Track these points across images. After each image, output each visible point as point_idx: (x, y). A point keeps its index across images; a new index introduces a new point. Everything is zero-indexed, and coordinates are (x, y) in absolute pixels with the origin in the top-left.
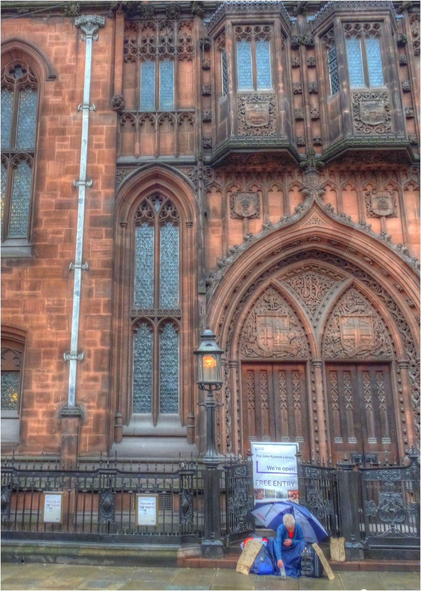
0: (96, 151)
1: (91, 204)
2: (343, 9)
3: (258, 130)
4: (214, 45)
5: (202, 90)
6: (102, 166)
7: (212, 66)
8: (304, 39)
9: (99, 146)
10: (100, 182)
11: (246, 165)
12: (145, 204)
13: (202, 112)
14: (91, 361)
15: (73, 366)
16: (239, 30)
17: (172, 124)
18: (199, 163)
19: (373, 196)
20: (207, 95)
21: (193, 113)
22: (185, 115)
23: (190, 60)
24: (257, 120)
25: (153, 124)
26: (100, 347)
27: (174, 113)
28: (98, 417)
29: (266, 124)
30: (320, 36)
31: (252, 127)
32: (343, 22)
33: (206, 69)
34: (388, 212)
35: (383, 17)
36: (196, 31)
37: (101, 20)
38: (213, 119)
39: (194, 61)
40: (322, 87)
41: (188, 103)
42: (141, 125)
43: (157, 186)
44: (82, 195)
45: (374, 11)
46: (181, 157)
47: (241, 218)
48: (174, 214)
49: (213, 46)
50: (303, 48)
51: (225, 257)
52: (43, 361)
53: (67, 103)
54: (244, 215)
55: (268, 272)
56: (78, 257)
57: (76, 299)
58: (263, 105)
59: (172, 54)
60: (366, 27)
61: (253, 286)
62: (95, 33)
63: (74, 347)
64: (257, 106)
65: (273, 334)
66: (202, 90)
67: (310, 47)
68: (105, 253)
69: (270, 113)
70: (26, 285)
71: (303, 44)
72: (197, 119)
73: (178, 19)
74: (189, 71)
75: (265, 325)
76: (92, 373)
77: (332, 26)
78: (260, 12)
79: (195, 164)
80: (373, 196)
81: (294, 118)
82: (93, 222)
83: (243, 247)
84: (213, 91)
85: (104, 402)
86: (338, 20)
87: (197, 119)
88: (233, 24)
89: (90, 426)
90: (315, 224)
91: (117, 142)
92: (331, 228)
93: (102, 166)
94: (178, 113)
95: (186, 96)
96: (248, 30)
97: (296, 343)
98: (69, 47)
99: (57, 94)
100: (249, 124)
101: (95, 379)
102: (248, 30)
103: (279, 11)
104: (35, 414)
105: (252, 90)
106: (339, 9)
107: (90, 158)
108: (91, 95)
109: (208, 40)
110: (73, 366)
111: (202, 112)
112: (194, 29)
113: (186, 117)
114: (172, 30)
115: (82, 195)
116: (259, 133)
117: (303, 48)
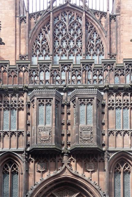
2: (79, 94)
3: (45, 141)
4: (32, 105)
5: (26, 122)
7: (31, 113)
8: (66, 102)
12: (6, 166)
13: (26, 132)
16: (40, 101)
17: (16, 136)
18: (25, 152)
19: (87, 164)
20: (29, 125)
21: (23, 132)
22: (21, 132)
23: (23, 110)
24: (45, 137)
25: (8, 136)
27: (16, 132)
29: (48, 139)
30: (72, 102)
31: (43, 140)
32: (79, 98)
33: (28, 114)
35: (94, 97)
36: (25, 98)
38: (30, 134)
39: (24, 110)
40: (71, 122)
41: (22, 128)
42: (4, 136)
43: (10, 159)
45: (91, 94)
46: (18, 148)
47: (40, 172)
48: (17, 169)
49: (31, 105)
50: (65, 106)
51: (33, 186)
54: (41, 171)
55: (50, 190)
58: (47, 132)
59: (16, 107)
60: (88, 100)
64: (45, 132)
66: (26, 122)
67: (69, 106)
69: (50, 135)
71: (66, 105)
72: (25, 134)
73: (18, 93)
74: (22, 114)
77: (75, 99)
78: (47, 94)
79: (23, 152)
80: (87, 164)
81: (60, 134)
83: (39, 182)
84: (31, 124)
86: (77, 98)
87: (25, 134)
88: (38, 99)
90: (67, 174)
92: (71, 175)
94: (18, 132)
95: (21, 124)
96: (43, 101)
100: (42, 139)
102: (43, 101)
103: (55, 94)
105: (43, 125)
106: (77, 94)
109: (29, 102)
111: (26, 132)
112: (24, 97)
113: (20, 133)
114: (16, 97)
116: (45, 142)
117: (65, 106)
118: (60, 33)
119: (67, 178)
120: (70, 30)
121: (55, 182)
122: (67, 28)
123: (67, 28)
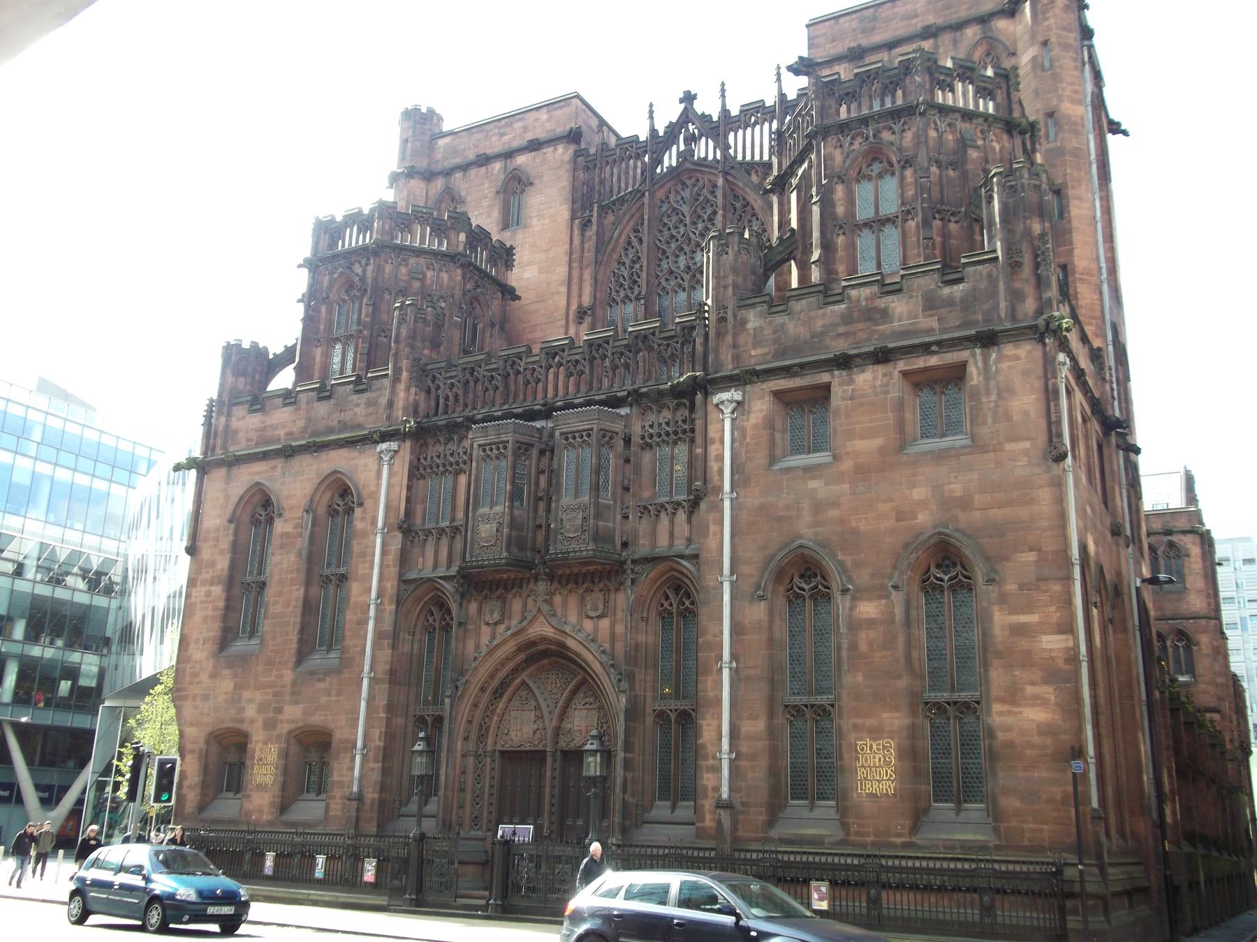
0: (386, 571)
1: (378, 620)
6: (389, 585)
9: (388, 566)
10: (386, 600)
11: (480, 583)
14: (371, 755)
15: (358, 759)
22: (457, 528)
26: (378, 743)
28: (373, 799)
34: (599, 613)
37: (394, 445)
44: (372, 613)
52: (342, 755)
53: (369, 527)
55: (516, 671)
56: (367, 668)
57: (363, 704)
61: (504, 685)
62: (391, 458)
63: (359, 744)
65: (521, 729)
68: (386, 663)
70: (334, 692)
75: (516, 718)
76: (372, 765)
82: (379, 635)
85: (377, 788)
89: (368, 807)
90: (542, 629)
91: (404, 559)
93: (389, 585)
97: (538, 735)
98: (373, 474)
99: (363, 519)
101: (373, 769)
104: (334, 798)
107: (381, 579)
108: (386, 517)
110: (358, 759)
115: (372, 613)
118: (672, 236)
119: (544, 639)
120: (694, 223)
121: (521, 648)
122: (688, 221)
123: (688, 221)
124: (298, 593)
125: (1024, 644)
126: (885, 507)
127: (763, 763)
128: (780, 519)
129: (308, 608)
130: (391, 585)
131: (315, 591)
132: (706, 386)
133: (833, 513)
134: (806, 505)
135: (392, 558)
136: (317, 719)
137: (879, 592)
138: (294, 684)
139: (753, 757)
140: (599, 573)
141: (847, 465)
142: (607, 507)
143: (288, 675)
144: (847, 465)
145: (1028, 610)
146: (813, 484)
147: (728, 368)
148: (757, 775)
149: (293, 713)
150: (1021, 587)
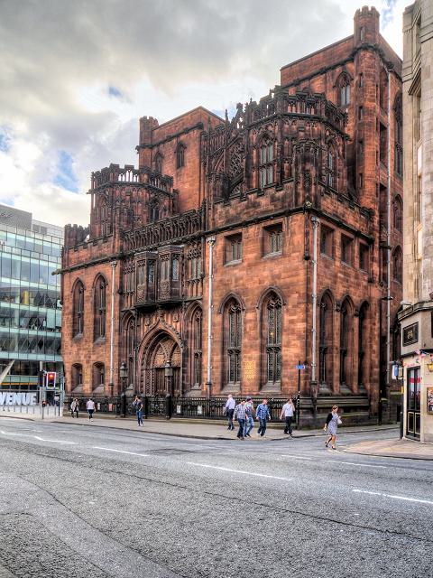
82: (115, 331)
90: (161, 326)
91: (121, 304)
124: (92, 317)
125: (292, 326)
126: (256, 279)
127: (220, 370)
128: (225, 285)
129: (95, 321)
130: (117, 313)
131: (98, 316)
132: (205, 235)
133: (241, 282)
134: (233, 279)
135: (117, 304)
136: (100, 360)
137: (253, 310)
138: (93, 348)
139: (217, 368)
140: (172, 307)
141: (245, 264)
142: (176, 282)
143: (92, 345)
144: (245, 264)
145: (294, 314)
146: (236, 271)
147: (211, 229)
148: (218, 374)
149: (94, 358)
150: (293, 306)
